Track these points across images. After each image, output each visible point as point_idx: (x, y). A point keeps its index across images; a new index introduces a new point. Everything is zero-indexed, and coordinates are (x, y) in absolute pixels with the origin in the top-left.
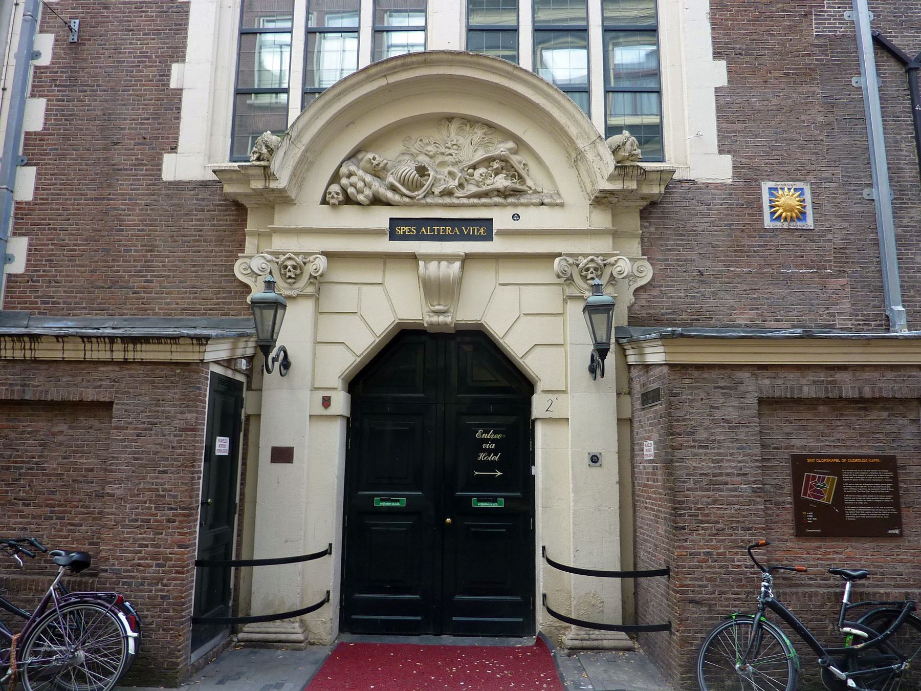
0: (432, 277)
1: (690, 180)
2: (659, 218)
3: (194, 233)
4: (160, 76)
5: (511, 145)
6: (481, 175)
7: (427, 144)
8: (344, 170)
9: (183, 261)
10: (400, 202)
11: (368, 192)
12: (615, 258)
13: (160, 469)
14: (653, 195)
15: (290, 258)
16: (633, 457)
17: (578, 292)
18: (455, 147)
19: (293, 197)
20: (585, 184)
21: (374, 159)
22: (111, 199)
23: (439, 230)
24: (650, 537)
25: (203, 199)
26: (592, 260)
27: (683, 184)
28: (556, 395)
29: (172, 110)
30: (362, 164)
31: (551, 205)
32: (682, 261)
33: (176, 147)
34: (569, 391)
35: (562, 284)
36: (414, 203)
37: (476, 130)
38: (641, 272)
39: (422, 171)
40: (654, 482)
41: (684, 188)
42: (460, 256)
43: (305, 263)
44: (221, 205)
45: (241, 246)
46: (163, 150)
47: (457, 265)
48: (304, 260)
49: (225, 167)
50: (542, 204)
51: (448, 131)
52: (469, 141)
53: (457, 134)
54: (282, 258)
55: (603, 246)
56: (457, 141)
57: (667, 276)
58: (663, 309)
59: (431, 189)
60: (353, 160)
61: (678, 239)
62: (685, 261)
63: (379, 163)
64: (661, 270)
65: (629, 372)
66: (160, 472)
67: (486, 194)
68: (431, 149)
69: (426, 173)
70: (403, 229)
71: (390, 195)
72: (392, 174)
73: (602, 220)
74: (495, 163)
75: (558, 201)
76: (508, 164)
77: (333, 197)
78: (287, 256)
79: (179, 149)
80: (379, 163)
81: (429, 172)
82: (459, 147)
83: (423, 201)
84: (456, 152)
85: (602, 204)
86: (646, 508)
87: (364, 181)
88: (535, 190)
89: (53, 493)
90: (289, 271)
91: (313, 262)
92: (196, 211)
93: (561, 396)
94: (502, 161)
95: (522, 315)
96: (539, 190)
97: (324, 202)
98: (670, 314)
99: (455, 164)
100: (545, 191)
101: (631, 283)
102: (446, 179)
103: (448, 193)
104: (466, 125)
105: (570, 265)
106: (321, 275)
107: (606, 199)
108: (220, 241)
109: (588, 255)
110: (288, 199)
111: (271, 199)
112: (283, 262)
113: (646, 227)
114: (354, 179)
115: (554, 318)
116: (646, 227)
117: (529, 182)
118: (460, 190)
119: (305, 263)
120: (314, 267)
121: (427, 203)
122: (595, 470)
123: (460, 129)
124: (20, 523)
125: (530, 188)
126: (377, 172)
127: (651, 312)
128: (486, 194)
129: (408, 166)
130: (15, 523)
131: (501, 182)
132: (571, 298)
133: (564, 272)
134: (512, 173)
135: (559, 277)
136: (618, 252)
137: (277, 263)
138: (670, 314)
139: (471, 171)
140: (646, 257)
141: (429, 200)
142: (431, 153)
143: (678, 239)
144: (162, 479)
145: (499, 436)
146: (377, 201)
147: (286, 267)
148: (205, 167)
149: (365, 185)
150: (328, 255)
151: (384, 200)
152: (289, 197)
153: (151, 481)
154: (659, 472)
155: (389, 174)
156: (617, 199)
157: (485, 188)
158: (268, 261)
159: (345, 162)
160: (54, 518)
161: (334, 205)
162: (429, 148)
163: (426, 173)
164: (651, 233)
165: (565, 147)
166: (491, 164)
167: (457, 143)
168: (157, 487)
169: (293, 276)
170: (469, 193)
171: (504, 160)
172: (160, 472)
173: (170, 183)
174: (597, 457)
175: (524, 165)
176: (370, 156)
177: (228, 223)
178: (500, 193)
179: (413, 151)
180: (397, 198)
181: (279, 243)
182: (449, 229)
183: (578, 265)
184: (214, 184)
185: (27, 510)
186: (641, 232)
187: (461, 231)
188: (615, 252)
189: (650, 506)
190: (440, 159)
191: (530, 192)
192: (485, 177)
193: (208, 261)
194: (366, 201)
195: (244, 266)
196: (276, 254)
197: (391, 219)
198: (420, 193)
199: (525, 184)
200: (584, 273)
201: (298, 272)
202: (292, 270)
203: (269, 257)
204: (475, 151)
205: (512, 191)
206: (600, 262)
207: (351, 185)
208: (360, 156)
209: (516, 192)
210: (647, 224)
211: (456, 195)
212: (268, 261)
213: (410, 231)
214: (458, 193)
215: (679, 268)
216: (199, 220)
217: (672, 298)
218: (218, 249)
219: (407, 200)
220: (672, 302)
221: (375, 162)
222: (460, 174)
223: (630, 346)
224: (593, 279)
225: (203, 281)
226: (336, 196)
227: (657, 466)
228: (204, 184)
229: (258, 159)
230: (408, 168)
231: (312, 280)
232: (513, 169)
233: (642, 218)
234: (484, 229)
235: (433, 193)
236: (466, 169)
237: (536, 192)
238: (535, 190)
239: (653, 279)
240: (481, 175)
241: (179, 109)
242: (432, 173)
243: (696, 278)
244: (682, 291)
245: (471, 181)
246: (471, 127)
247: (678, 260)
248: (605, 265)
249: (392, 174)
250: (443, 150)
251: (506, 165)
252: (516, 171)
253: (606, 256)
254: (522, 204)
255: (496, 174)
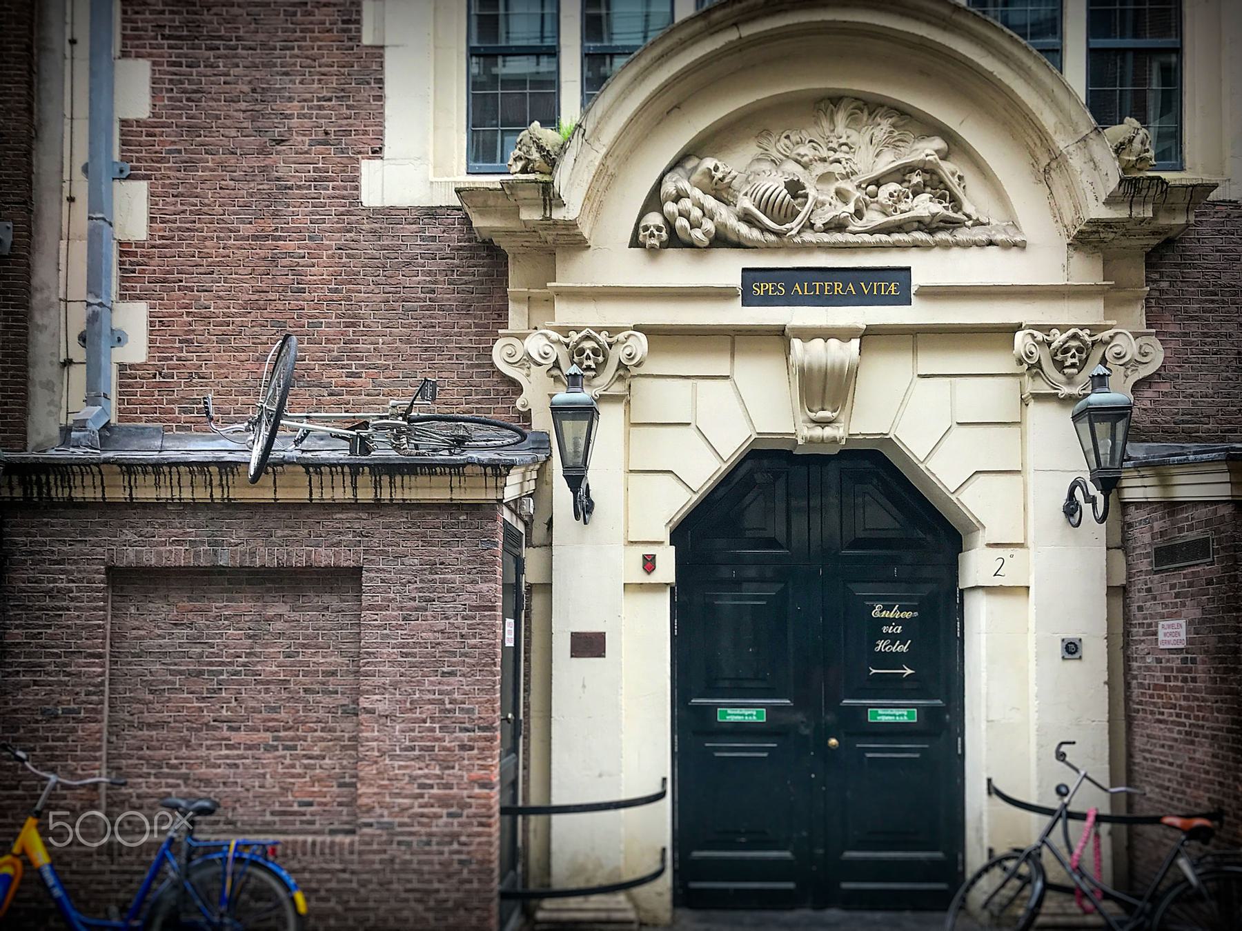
0: (816, 367)
1: (1230, 201)
2: (1177, 265)
3: (422, 295)
4: (344, 22)
5: (938, 143)
6: (891, 195)
7: (798, 143)
8: (669, 187)
9: (409, 342)
10: (759, 241)
11: (709, 225)
12: (1111, 332)
13: (445, 669)
14: (1171, 228)
15: (588, 338)
16: (1128, 644)
17: (1047, 387)
18: (844, 148)
19: (586, 235)
20: (1062, 210)
21: (716, 169)
22: (279, 238)
23: (822, 288)
24: (1171, 764)
25: (433, 239)
26: (1075, 337)
27: (1217, 208)
28: (1010, 551)
29: (369, 83)
30: (696, 177)
31: (1008, 246)
32: (1211, 337)
33: (381, 148)
34: (1030, 543)
35: (1022, 375)
36: (783, 244)
37: (878, 119)
38: (1145, 355)
39: (795, 188)
40: (1185, 680)
41: (1219, 215)
42: (858, 329)
43: (610, 345)
44: (461, 249)
45: (501, 317)
46: (360, 153)
47: (855, 343)
48: (610, 340)
49: (464, 183)
50: (991, 243)
51: (832, 121)
52: (867, 139)
53: (847, 127)
54: (575, 337)
55: (1086, 313)
56: (848, 137)
57: (1187, 361)
58: (1177, 414)
59: (809, 219)
60: (680, 170)
61: (1206, 301)
62: (1216, 336)
63: (724, 177)
64: (1176, 352)
65: (1124, 514)
66: (444, 674)
67: (899, 228)
68: (806, 150)
69: (800, 192)
70: (765, 286)
71: (744, 229)
72: (746, 194)
73: (1085, 272)
74: (914, 175)
75: (1018, 238)
76: (935, 177)
77: (652, 235)
78: (583, 333)
79: (387, 152)
80: (724, 177)
81: (807, 191)
82: (850, 148)
83: (797, 240)
84: (847, 156)
85: (1089, 243)
86: (1160, 721)
87: (702, 208)
88: (978, 219)
89: (274, 710)
90: (588, 358)
91: (623, 343)
92: (421, 258)
93: (1018, 551)
94: (925, 171)
95: (955, 425)
96: (984, 219)
97: (635, 243)
98: (1187, 422)
99: (847, 176)
100: (993, 222)
101: (1129, 372)
102: (834, 202)
103: (838, 226)
104: (862, 111)
105: (1038, 343)
106: (638, 365)
107: (1097, 235)
108: (466, 307)
109: (1068, 327)
110: (578, 238)
111: (550, 239)
112: (577, 342)
113: (1155, 281)
114: (686, 204)
115: (1005, 429)
116: (1155, 281)
117: (968, 208)
118: (857, 220)
119: (610, 345)
120: (628, 351)
121: (803, 242)
122: (1072, 665)
123: (853, 120)
124: (227, 757)
125: (969, 217)
126: (721, 190)
127: (1159, 420)
128: (899, 228)
129: (773, 180)
130: (221, 757)
131: (925, 206)
132: (1038, 397)
133: (1029, 355)
134: (939, 192)
135: (1020, 362)
136: (1114, 322)
137: (567, 345)
138: (1187, 422)
139: (872, 188)
140: (1154, 331)
141: (809, 236)
142: (806, 159)
143: (1206, 301)
144: (448, 685)
145: (907, 615)
146: (722, 241)
147: (581, 352)
148: (432, 183)
149: (704, 215)
150: (651, 332)
151: (734, 238)
152: (581, 235)
153: (431, 688)
154: (1200, 667)
155: (741, 195)
156: (1112, 236)
157: (898, 217)
158: (553, 342)
159: (669, 175)
160: (280, 747)
161: (652, 247)
162: (802, 150)
163: (800, 192)
164: (1161, 291)
165: (1028, 147)
166: (907, 178)
167: (848, 141)
168: (440, 697)
169: (594, 366)
170: (873, 224)
171: (928, 170)
172: (444, 674)
173: (376, 211)
174: (1076, 646)
175: (960, 178)
176: (709, 163)
177: (476, 278)
178: (922, 225)
179: (775, 154)
180: (755, 234)
181: (566, 313)
182: (838, 286)
183: (1049, 344)
184: (449, 212)
185: (236, 737)
186: (1148, 289)
187: (859, 290)
188: (1109, 323)
189: (1174, 718)
190: (820, 169)
191: (969, 223)
192: (896, 198)
193: (448, 342)
194: (706, 241)
195: (509, 350)
196: (565, 331)
197: (744, 270)
198: (795, 225)
199: (960, 209)
200: (1059, 357)
201: (601, 359)
202: (591, 355)
203: (555, 336)
204: (877, 155)
205: (941, 221)
206: (1087, 338)
207: (681, 215)
208: (690, 165)
209: (950, 224)
210: (1156, 276)
211: (850, 228)
212: (553, 342)
213: (776, 289)
214: (856, 225)
215: (1206, 348)
216: (429, 273)
217: (1192, 396)
218: (463, 322)
219: (772, 238)
220: (1193, 402)
221: (719, 175)
222: (858, 194)
223: (1136, 474)
224: (1073, 366)
225: (444, 375)
226: (656, 233)
227: (1195, 658)
228: (432, 213)
229: (524, 170)
230: (773, 183)
231: (621, 372)
232: (941, 186)
233: (1150, 266)
234: (895, 285)
235: (812, 226)
236: (863, 186)
237: (977, 223)
238: (978, 219)
239: (1163, 367)
240: (891, 195)
241: (381, 81)
242: (811, 192)
243: (1234, 363)
244: (1210, 385)
245: (872, 206)
246: (870, 114)
247: (1205, 335)
248: (1094, 343)
249: (746, 194)
250: (824, 153)
251: (931, 178)
252: (947, 188)
253: (1094, 329)
254: (957, 244)
255: (915, 194)
